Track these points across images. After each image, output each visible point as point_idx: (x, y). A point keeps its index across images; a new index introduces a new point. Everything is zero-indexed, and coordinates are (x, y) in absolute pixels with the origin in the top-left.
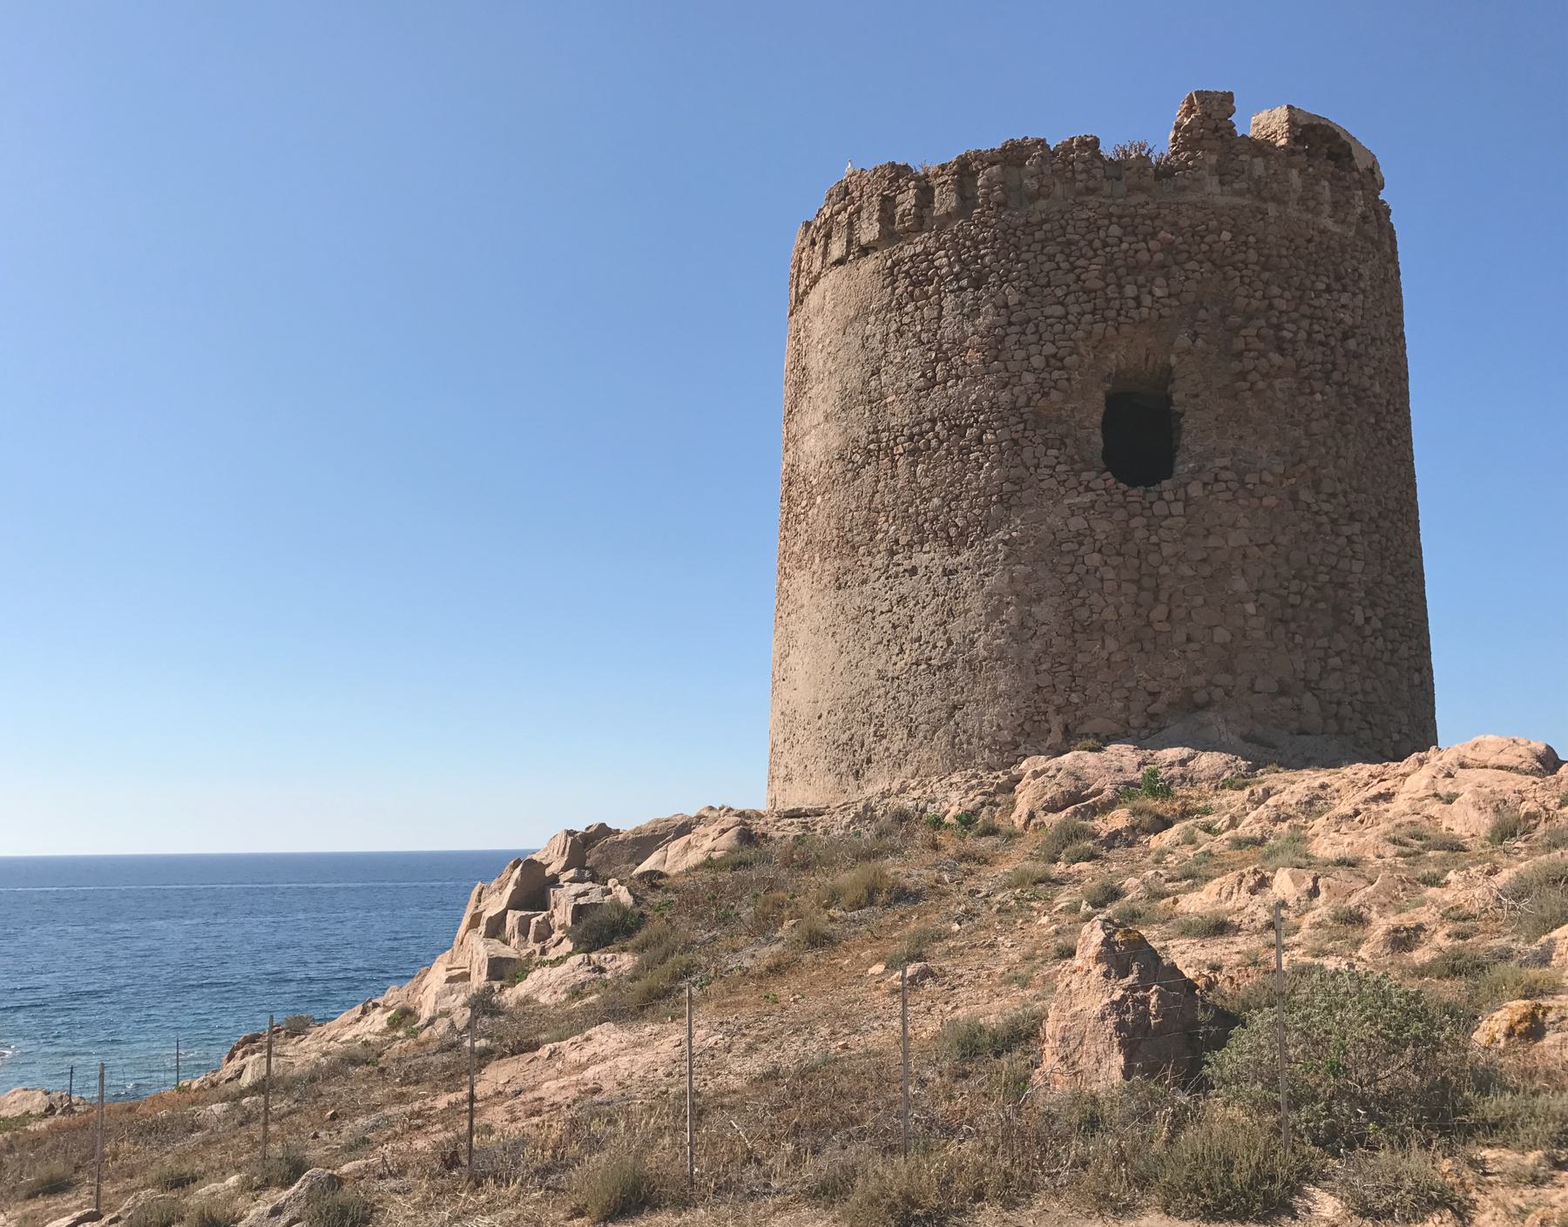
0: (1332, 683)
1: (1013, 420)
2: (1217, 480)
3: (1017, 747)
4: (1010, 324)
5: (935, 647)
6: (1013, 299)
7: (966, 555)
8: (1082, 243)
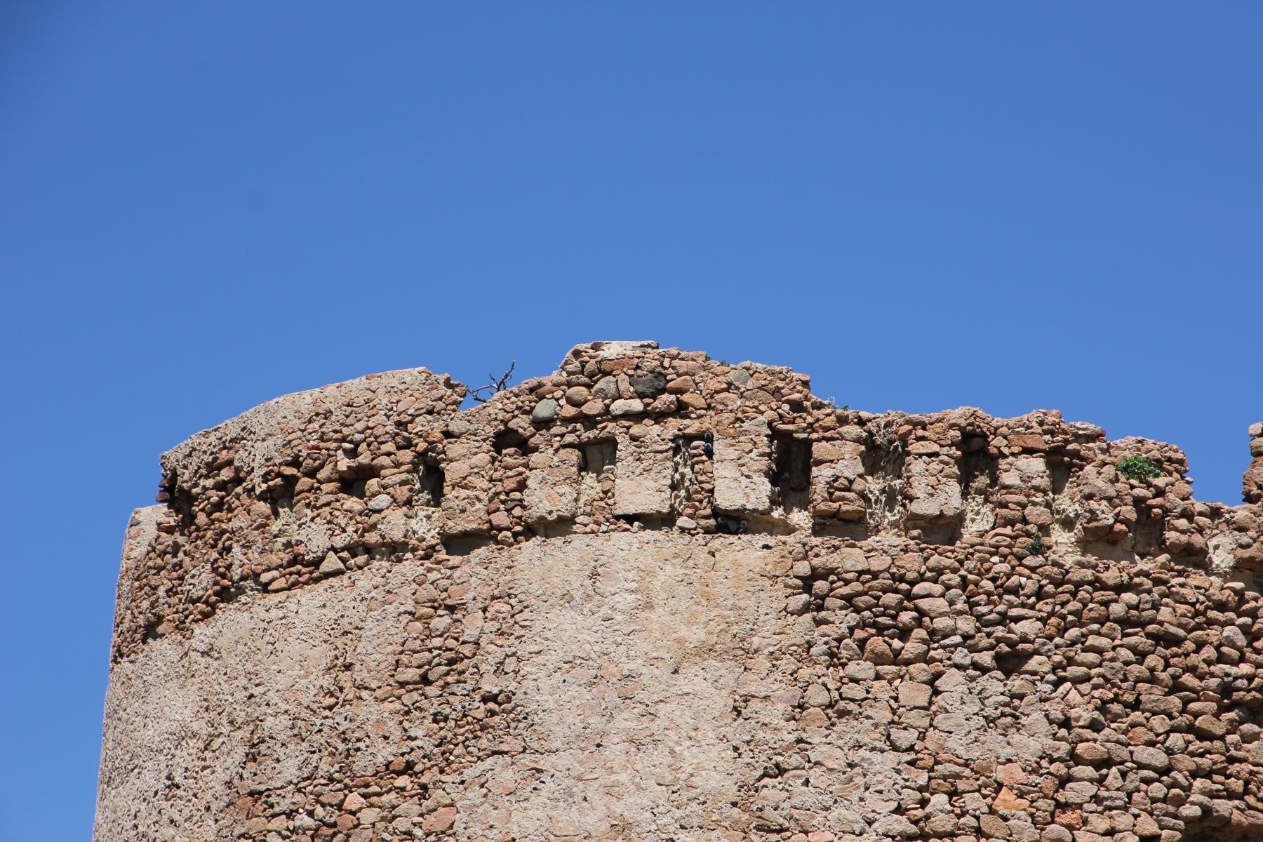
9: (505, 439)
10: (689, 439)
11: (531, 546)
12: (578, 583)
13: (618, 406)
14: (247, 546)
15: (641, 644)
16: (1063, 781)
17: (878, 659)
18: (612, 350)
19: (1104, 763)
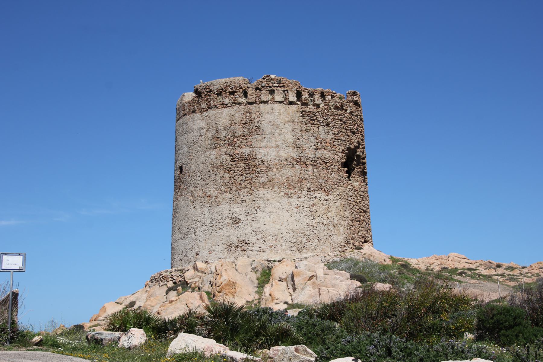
4: (335, 139)
7: (330, 197)
9: (257, 89)
10: (285, 91)
11: (262, 105)
12: (270, 111)
13: (275, 85)
14: (214, 101)
15: (279, 120)
16: (334, 142)
17: (311, 124)
18: (273, 76)
19: (338, 140)
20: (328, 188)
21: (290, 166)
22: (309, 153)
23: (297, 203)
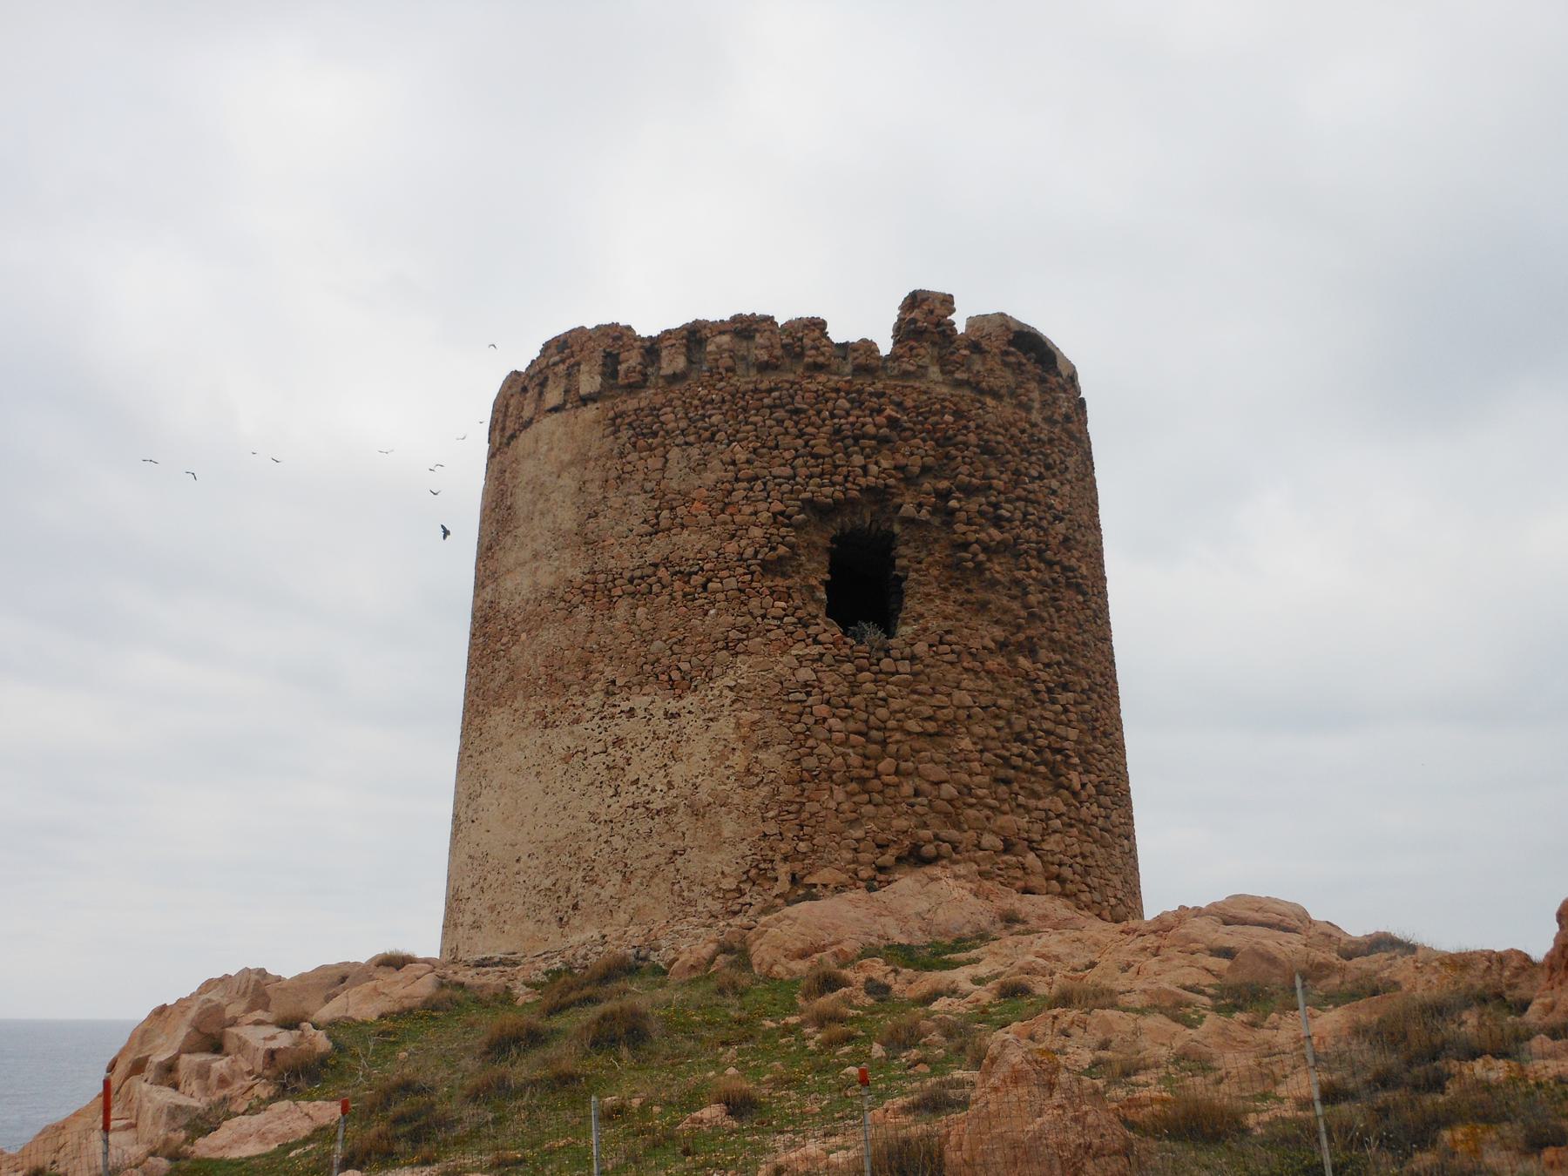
0: (1051, 844)
1: (741, 571)
2: (941, 643)
3: (742, 893)
4: (737, 480)
5: (654, 790)
6: (741, 456)
7: (690, 699)
8: (811, 412)
16: (730, 493)
20: (685, 666)
21: (561, 614)
22: (622, 558)
23: (568, 741)
